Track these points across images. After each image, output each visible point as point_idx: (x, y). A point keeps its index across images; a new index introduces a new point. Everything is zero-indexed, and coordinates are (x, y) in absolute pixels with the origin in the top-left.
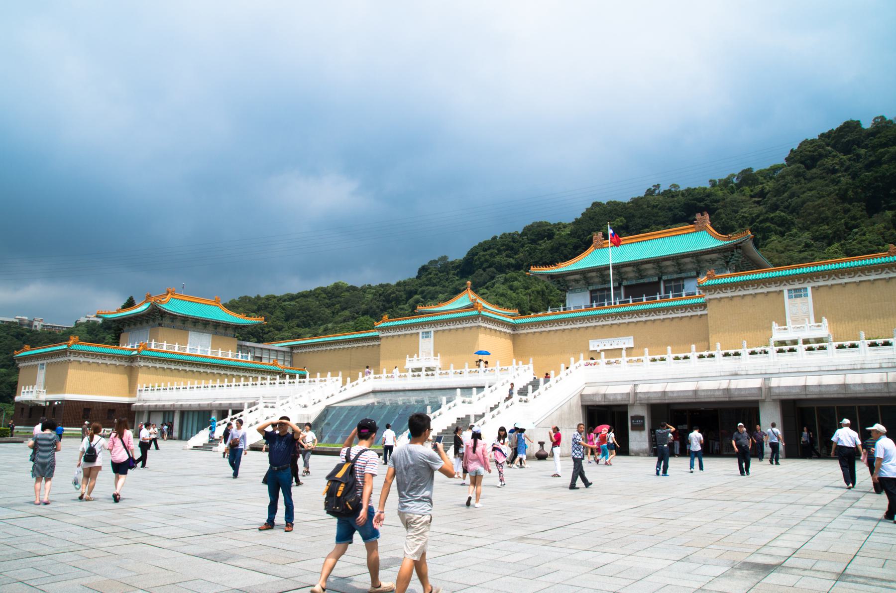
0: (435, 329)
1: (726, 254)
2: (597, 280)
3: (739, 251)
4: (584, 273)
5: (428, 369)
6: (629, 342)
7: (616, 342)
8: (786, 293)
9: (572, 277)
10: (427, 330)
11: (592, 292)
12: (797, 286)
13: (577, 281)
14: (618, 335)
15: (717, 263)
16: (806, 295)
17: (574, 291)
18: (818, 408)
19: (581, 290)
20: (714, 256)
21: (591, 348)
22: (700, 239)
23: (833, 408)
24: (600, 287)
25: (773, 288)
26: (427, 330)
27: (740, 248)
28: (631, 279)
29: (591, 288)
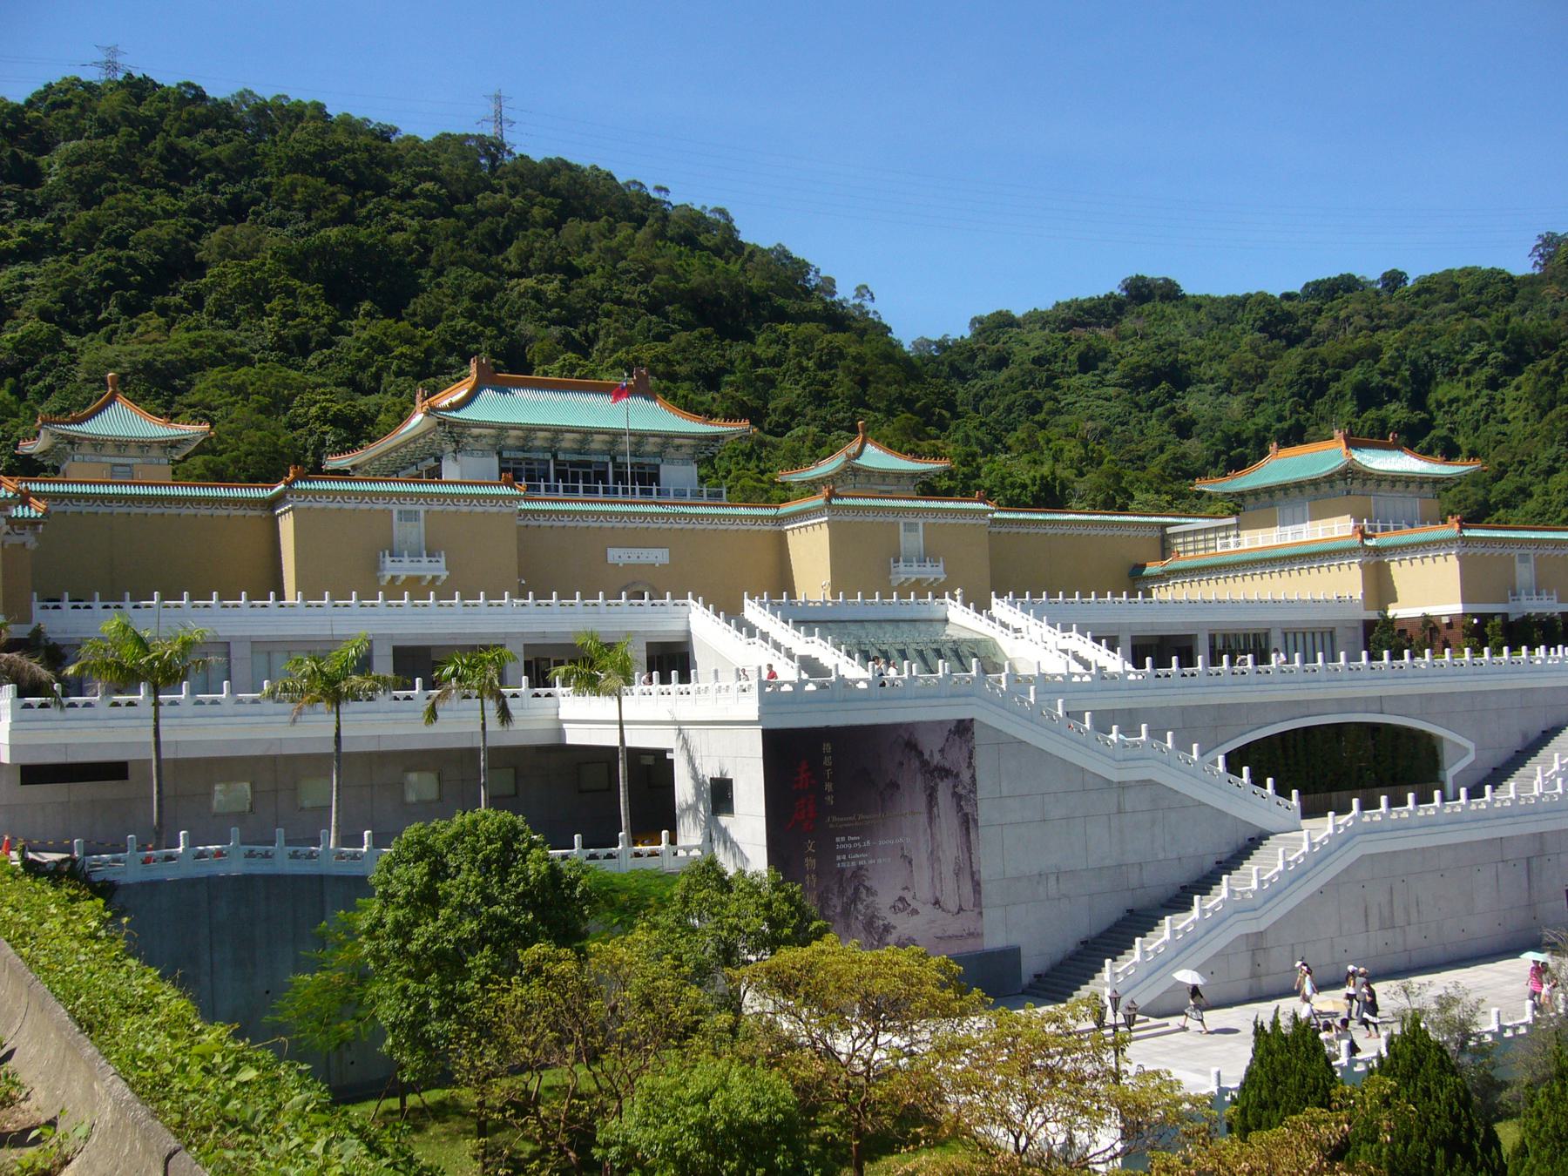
0: (425, 507)
9: (476, 431)
10: (408, 506)
11: (501, 460)
25: (891, 519)
29: (506, 454)
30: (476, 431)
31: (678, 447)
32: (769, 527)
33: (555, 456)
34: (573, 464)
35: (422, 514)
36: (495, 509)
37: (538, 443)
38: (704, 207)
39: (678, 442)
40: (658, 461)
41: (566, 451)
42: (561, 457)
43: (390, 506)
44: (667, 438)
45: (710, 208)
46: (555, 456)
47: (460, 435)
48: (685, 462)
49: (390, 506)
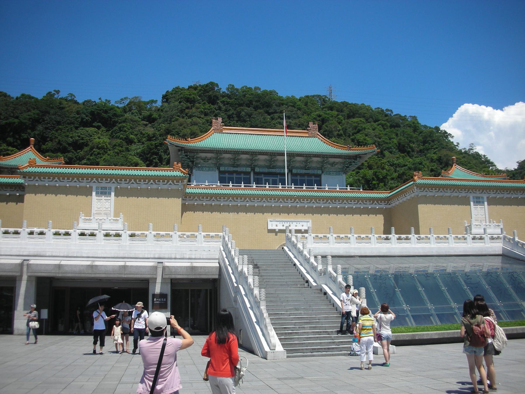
1: (350, 161)
4: (218, 152)
7: (295, 223)
9: (203, 155)
10: (104, 185)
11: (220, 172)
12: (478, 194)
15: (336, 166)
17: (201, 168)
18: (191, 290)
19: (210, 169)
21: (270, 227)
22: (312, 143)
23: (188, 290)
25: (463, 194)
26: (104, 185)
27: (360, 157)
29: (222, 169)
30: (203, 155)
31: (333, 164)
32: (383, 206)
33: (253, 169)
34: (265, 174)
35: (113, 189)
36: (166, 187)
37: (243, 163)
38: (406, 116)
39: (332, 160)
40: (319, 172)
41: (260, 167)
42: (257, 170)
44: (324, 157)
45: (408, 116)
46: (253, 169)
47: (193, 157)
49: (92, 184)
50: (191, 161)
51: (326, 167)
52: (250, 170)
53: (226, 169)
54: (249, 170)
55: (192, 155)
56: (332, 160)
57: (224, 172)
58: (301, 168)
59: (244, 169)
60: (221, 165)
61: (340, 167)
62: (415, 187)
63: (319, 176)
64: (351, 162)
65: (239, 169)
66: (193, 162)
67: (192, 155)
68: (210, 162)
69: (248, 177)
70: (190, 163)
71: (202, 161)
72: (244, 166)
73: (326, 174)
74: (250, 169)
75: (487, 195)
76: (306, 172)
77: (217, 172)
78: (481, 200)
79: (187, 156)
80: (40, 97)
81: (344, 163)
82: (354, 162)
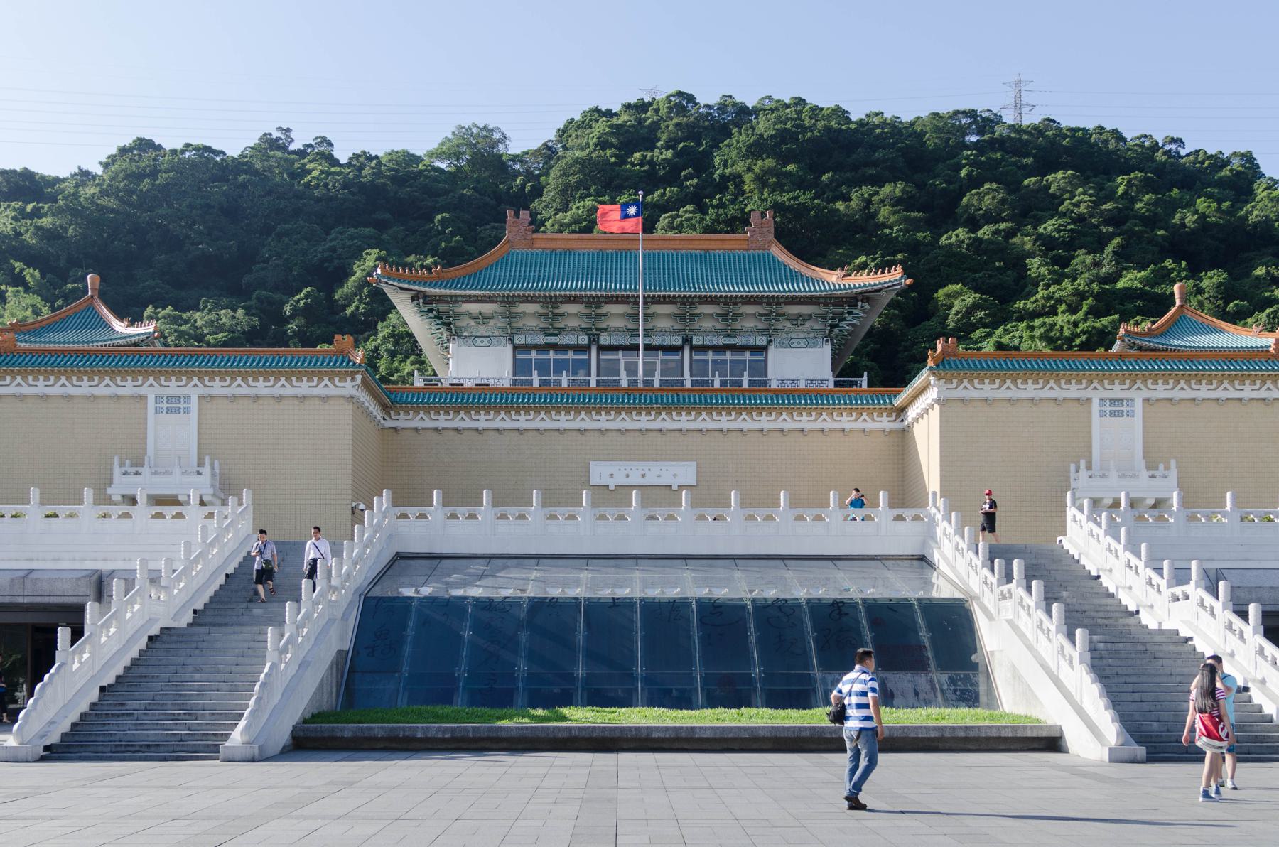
0: (201, 390)
1: (839, 309)
2: (531, 323)
3: (867, 306)
5: (158, 500)
6: (682, 473)
8: (1096, 407)
11: (516, 348)
13: (482, 319)
14: (659, 456)
15: (808, 324)
16: (1131, 414)
20: (806, 310)
24: (542, 340)
27: (868, 300)
28: (663, 332)
29: (519, 340)
35: (194, 399)
37: (573, 323)
40: (761, 341)
43: (144, 390)
48: (809, 343)
50: (443, 324)
51: (780, 326)
52: (586, 342)
53: (530, 340)
54: (584, 340)
55: (443, 308)
56: (794, 310)
57: (526, 348)
58: (718, 332)
59: (571, 340)
60: (519, 330)
61: (816, 326)
62: (932, 378)
63: (763, 349)
64: (842, 314)
65: (560, 340)
66: (448, 325)
67: (443, 308)
68: (492, 323)
69: (586, 357)
70: (443, 329)
71: (472, 323)
72: (574, 331)
73: (782, 344)
74: (586, 338)
75: (1146, 394)
76: (727, 341)
77: (509, 348)
78: (1125, 409)
79: (431, 311)
80: (234, 151)
81: (823, 316)
82: (850, 313)
